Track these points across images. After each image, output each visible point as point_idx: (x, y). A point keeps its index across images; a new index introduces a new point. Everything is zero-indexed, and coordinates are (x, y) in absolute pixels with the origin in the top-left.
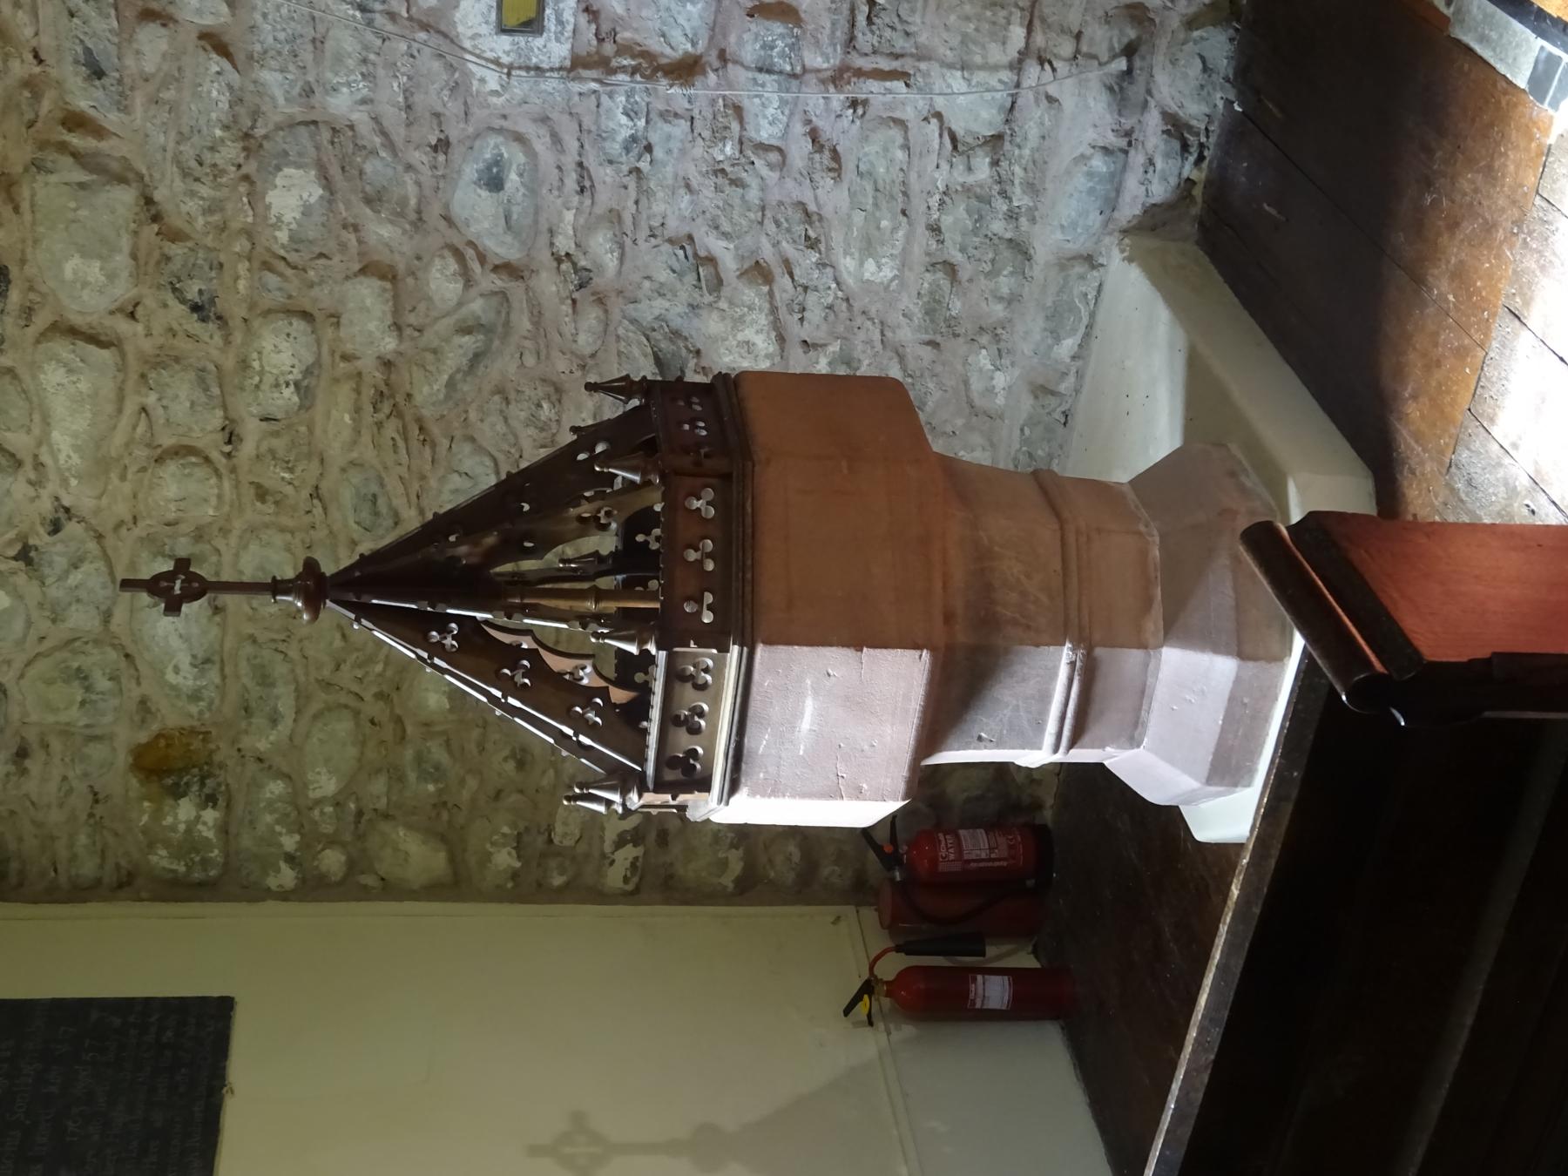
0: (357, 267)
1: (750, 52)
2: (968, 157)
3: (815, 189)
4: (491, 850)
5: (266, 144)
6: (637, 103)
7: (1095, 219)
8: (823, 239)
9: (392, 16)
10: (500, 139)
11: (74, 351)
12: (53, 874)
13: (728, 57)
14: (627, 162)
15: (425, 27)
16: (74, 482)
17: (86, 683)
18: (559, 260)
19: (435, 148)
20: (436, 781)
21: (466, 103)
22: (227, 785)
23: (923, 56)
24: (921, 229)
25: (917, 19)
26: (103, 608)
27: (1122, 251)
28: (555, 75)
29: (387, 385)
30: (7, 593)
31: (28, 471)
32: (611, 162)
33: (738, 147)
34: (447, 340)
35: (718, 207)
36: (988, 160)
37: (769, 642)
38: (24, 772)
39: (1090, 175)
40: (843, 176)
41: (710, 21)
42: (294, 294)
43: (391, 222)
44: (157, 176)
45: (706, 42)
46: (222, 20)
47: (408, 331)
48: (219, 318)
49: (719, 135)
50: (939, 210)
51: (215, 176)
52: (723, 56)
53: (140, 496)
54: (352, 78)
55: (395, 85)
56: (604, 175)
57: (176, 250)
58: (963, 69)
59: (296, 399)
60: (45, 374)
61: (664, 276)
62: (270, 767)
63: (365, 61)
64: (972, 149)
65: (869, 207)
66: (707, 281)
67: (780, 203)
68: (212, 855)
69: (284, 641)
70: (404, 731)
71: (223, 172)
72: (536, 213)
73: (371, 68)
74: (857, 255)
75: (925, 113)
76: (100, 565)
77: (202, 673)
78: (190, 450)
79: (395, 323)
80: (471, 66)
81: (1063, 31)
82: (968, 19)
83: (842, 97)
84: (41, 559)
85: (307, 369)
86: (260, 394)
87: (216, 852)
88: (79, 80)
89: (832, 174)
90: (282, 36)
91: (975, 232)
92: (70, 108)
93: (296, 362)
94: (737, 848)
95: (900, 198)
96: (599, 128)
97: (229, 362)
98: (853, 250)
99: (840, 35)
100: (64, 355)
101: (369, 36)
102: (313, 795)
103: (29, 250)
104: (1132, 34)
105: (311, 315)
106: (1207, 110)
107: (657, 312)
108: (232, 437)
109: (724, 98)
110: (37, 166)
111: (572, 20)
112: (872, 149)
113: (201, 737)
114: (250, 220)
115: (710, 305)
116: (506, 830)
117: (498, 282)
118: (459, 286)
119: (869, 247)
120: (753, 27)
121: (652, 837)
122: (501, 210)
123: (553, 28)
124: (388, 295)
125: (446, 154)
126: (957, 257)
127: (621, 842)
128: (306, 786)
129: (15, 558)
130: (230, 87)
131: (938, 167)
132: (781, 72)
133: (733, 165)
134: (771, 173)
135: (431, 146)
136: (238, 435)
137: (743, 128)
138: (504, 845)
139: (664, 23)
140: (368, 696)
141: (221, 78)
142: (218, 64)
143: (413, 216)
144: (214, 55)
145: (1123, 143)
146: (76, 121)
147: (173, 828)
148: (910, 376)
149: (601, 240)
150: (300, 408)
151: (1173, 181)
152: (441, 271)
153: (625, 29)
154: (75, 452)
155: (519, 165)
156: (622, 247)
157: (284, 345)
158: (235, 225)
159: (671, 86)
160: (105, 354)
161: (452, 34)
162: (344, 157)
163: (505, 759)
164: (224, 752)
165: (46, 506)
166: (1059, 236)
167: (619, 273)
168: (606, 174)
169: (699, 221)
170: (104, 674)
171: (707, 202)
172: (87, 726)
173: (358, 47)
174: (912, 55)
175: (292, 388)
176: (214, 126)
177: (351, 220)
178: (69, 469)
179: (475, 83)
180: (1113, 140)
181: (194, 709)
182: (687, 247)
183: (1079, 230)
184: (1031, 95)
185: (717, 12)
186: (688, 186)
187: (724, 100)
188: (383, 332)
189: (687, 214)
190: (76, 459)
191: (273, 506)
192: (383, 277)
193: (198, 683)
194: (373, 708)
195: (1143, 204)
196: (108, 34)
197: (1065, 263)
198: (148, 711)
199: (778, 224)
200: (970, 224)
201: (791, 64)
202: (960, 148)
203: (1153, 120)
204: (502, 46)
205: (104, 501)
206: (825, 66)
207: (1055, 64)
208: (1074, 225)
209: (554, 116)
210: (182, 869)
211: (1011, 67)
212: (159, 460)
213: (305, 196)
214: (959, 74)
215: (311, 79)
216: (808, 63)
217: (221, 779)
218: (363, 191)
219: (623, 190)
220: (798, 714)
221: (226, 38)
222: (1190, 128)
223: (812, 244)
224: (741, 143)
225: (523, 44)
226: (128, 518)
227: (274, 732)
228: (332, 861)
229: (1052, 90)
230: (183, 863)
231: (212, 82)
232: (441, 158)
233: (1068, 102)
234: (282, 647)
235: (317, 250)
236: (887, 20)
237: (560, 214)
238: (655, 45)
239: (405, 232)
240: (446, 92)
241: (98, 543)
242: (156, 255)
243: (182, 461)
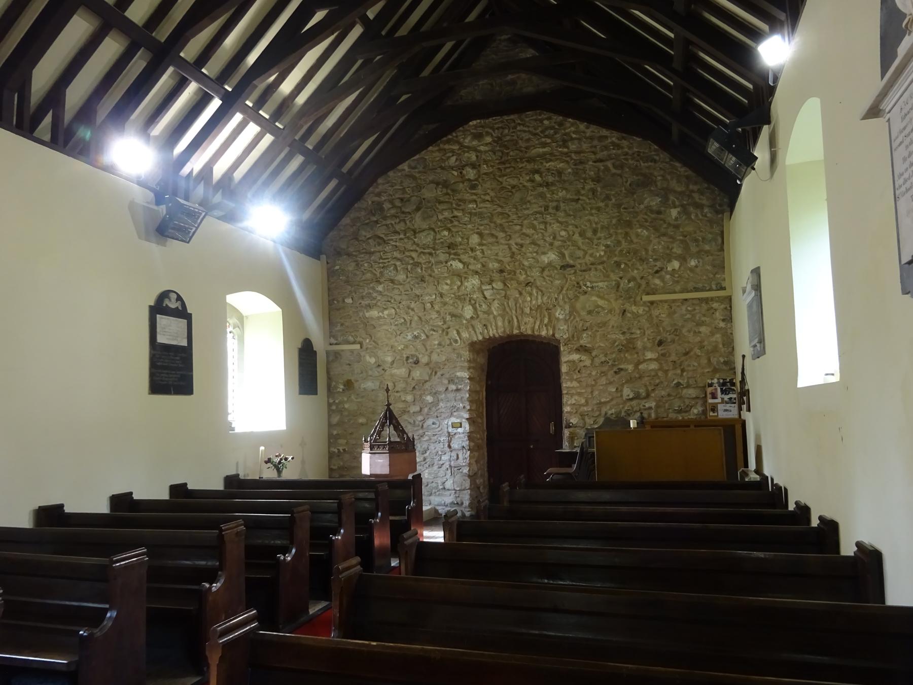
1: (452, 454)
7: (436, 503)
18: (424, 433)
31: (391, 366)
38: (347, 365)
49: (442, 452)
52: (451, 451)
56: (436, 437)
57: (421, 384)
61: (423, 447)
78: (395, 387)
81: (459, 495)
97: (408, 391)
99: (456, 466)
108: (397, 392)
110: (430, 368)
117: (421, 425)
119: (429, 474)
126: (429, 486)
127: (338, 449)
146: (436, 373)
160: (407, 376)
165: (386, 368)
197: (430, 501)
223: (429, 466)
228: (334, 407)
238: (452, 442)
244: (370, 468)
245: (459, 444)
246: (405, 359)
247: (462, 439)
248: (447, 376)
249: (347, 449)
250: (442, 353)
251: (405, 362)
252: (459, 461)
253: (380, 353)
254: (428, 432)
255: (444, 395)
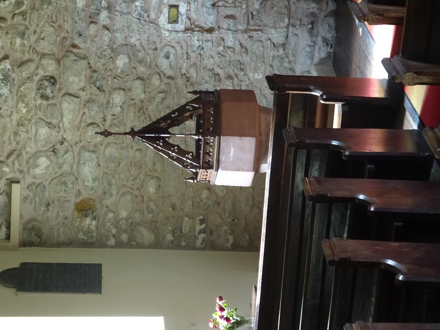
0: (136, 78)
1: (225, 26)
2: (278, 49)
3: (242, 57)
4: (166, 234)
5: (116, 50)
6: (200, 38)
7: (309, 62)
8: (244, 69)
9: (145, 21)
10: (169, 47)
11: (70, 99)
12: (53, 240)
13: (220, 27)
14: (198, 52)
15: (152, 23)
16: (67, 131)
17: (66, 185)
18: (182, 75)
19: (154, 50)
20: (152, 214)
21: (161, 39)
22: (99, 215)
23: (265, 25)
24: (268, 66)
25: (263, 17)
26: (71, 165)
27: (314, 69)
28: (181, 32)
29: (142, 106)
30: (49, 161)
32: (194, 52)
33: (223, 48)
34: (156, 95)
35: (219, 62)
36: (282, 49)
37: (223, 136)
38: (48, 210)
39: (306, 52)
40: (248, 53)
41: (216, 19)
42: (121, 84)
43: (144, 67)
44: (92, 58)
45: (215, 24)
46: (108, 23)
47: (147, 93)
48: (103, 91)
49: (219, 45)
50: (272, 61)
51: (105, 57)
52: (219, 27)
53: (82, 135)
54: (136, 34)
55: (145, 36)
56: (193, 55)
57: (95, 75)
58: (275, 28)
59: (120, 110)
60: (63, 104)
61: (207, 78)
62: (110, 209)
63: (139, 31)
64: (278, 47)
65: (255, 61)
66: (217, 79)
67: (234, 60)
68: (94, 234)
69: (115, 174)
70: (144, 199)
71: (106, 56)
72: (177, 64)
73: (140, 32)
74: (253, 72)
75: (267, 39)
76: (71, 153)
77: (94, 182)
78: (94, 124)
79: (144, 91)
80: (162, 31)
81: (297, 19)
82: (275, 17)
83: (247, 35)
84: (58, 152)
85: (123, 102)
86: (112, 109)
87: (95, 233)
88: (76, 37)
89: (246, 53)
90: (121, 26)
91: (281, 66)
92: (73, 43)
93: (121, 101)
94: (231, 235)
95: (262, 59)
96: (191, 44)
98: (252, 71)
100: (68, 100)
101: (140, 25)
102: (121, 217)
103: (62, 75)
104: (312, 19)
105: (125, 89)
106: (331, 36)
107: (206, 87)
109: (220, 37)
111: (185, 20)
112: (255, 47)
113: (93, 200)
114: (112, 67)
115: (218, 85)
116: (170, 228)
117: (169, 81)
118: (159, 81)
119: (256, 70)
120: (226, 21)
121: (208, 232)
122: (169, 63)
123: (181, 22)
124: (143, 84)
125: (156, 51)
127: (200, 233)
128: (118, 215)
129: (51, 152)
130: (109, 37)
131: (271, 51)
132: (232, 30)
133: (222, 52)
134: (232, 54)
135: (153, 49)
136: (106, 120)
137: (224, 43)
138: (169, 233)
139: (205, 20)
140: (135, 189)
141: (107, 35)
142: (107, 32)
143: (149, 65)
144: (106, 30)
145: (313, 44)
146: (74, 46)
147: (84, 227)
148: (268, 102)
149: (192, 70)
150: (121, 112)
151: (326, 52)
152: (155, 78)
153: (197, 22)
154: (68, 124)
155: (173, 53)
156: (197, 71)
157: (118, 97)
158: (108, 68)
159: (207, 34)
160: (77, 99)
161: (158, 24)
162: (133, 52)
163: (170, 207)
164: (98, 206)
165: (60, 138)
166: (301, 66)
167: (197, 78)
168: (193, 55)
169: (215, 65)
170: (70, 183)
171: (217, 61)
172: (65, 197)
173: (137, 28)
174: (263, 26)
175: (120, 107)
176: (105, 46)
177: (135, 67)
178: (67, 128)
179: (163, 35)
180: (310, 43)
181: (91, 193)
182: (212, 71)
183: (305, 65)
184: (291, 34)
185: (217, 17)
186: (212, 57)
187: (220, 37)
188: (141, 93)
189: (212, 63)
190: (68, 125)
191: (114, 137)
192: (142, 80)
193: (93, 185)
194: (136, 192)
195: (319, 58)
196: (84, 27)
198: (80, 193)
199: (234, 65)
200: (279, 64)
201: (235, 29)
202: (276, 46)
203: (320, 39)
204: (169, 26)
205: (74, 137)
206: (243, 28)
207: (296, 26)
208: (304, 64)
209: (181, 41)
210: (86, 238)
211: (286, 27)
212: (88, 126)
213: (125, 61)
214: (274, 29)
215: (126, 35)
216: (239, 28)
217: (97, 213)
218: (138, 60)
219: (197, 58)
220: (230, 152)
221: (108, 27)
222: (328, 40)
223: (242, 70)
224: (224, 46)
225: (174, 26)
226: (79, 141)
227: (111, 199)
228: (124, 237)
229: (296, 32)
230: (86, 237)
231: (105, 36)
232: (155, 52)
233: (300, 35)
234: (114, 175)
235: (127, 74)
236: (256, 18)
237: (183, 64)
238: (203, 25)
239: (147, 69)
240: (157, 37)
241: (71, 147)
242: (90, 76)
243: (93, 126)
244: (243, 170)
245: (209, 14)
246: (45, 102)
247: (200, 6)
248: (81, 25)
249: (201, 217)
250: (38, 31)
251: (50, 102)
252: (237, 15)
253: (31, 149)
254: (181, 69)
255: (118, 35)
